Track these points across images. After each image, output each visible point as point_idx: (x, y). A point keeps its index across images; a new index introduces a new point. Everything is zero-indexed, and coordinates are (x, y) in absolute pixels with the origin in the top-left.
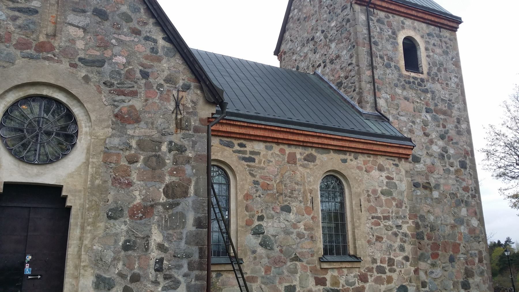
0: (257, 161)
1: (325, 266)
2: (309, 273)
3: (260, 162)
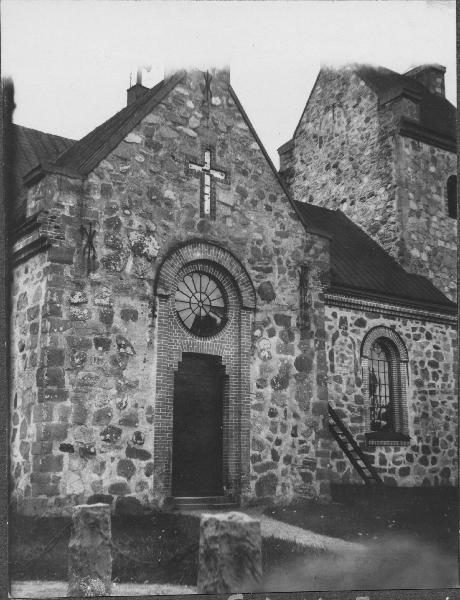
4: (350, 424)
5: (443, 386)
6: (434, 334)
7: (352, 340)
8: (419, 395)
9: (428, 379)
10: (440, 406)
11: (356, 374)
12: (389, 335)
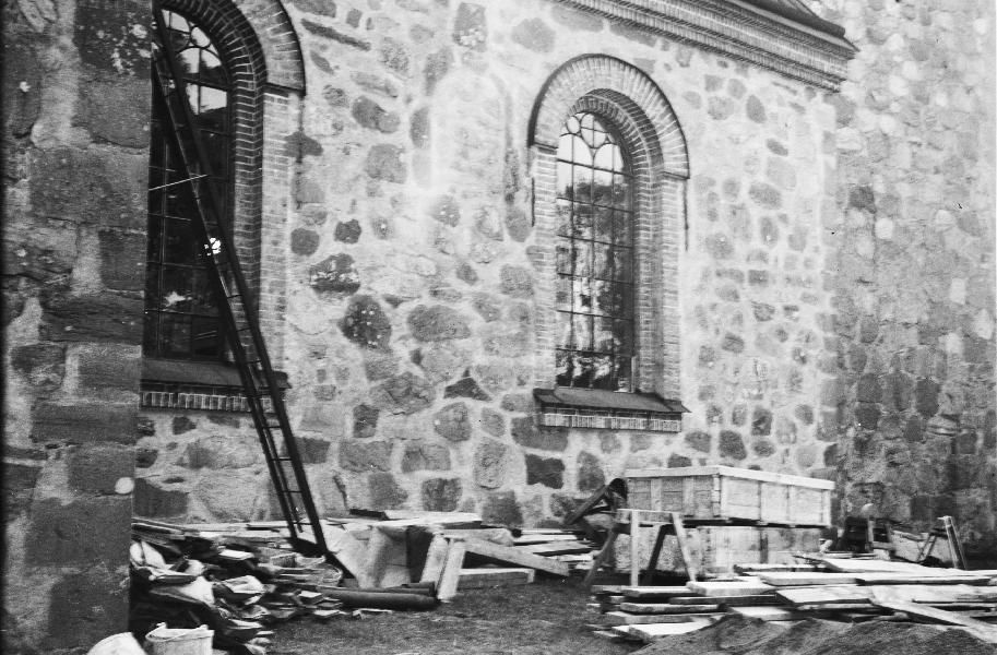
1: (556, 419)
2: (507, 439)
4: (480, 358)
5: (790, 264)
6: (771, 108)
8: (715, 282)
9: (747, 237)
10: (779, 319)
11: (510, 198)
12: (634, 89)
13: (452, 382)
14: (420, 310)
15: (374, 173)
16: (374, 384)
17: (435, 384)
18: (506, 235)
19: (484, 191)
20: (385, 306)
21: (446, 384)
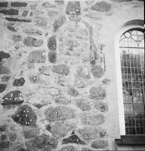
0: (20, 13)
3: (25, 14)
4: (80, 126)
7: (87, 25)
13: (67, 137)
14: (50, 109)
15: (31, 60)
16: (27, 140)
17: (57, 138)
18: (92, 75)
19: (81, 61)
20: (33, 108)
21: (63, 138)
